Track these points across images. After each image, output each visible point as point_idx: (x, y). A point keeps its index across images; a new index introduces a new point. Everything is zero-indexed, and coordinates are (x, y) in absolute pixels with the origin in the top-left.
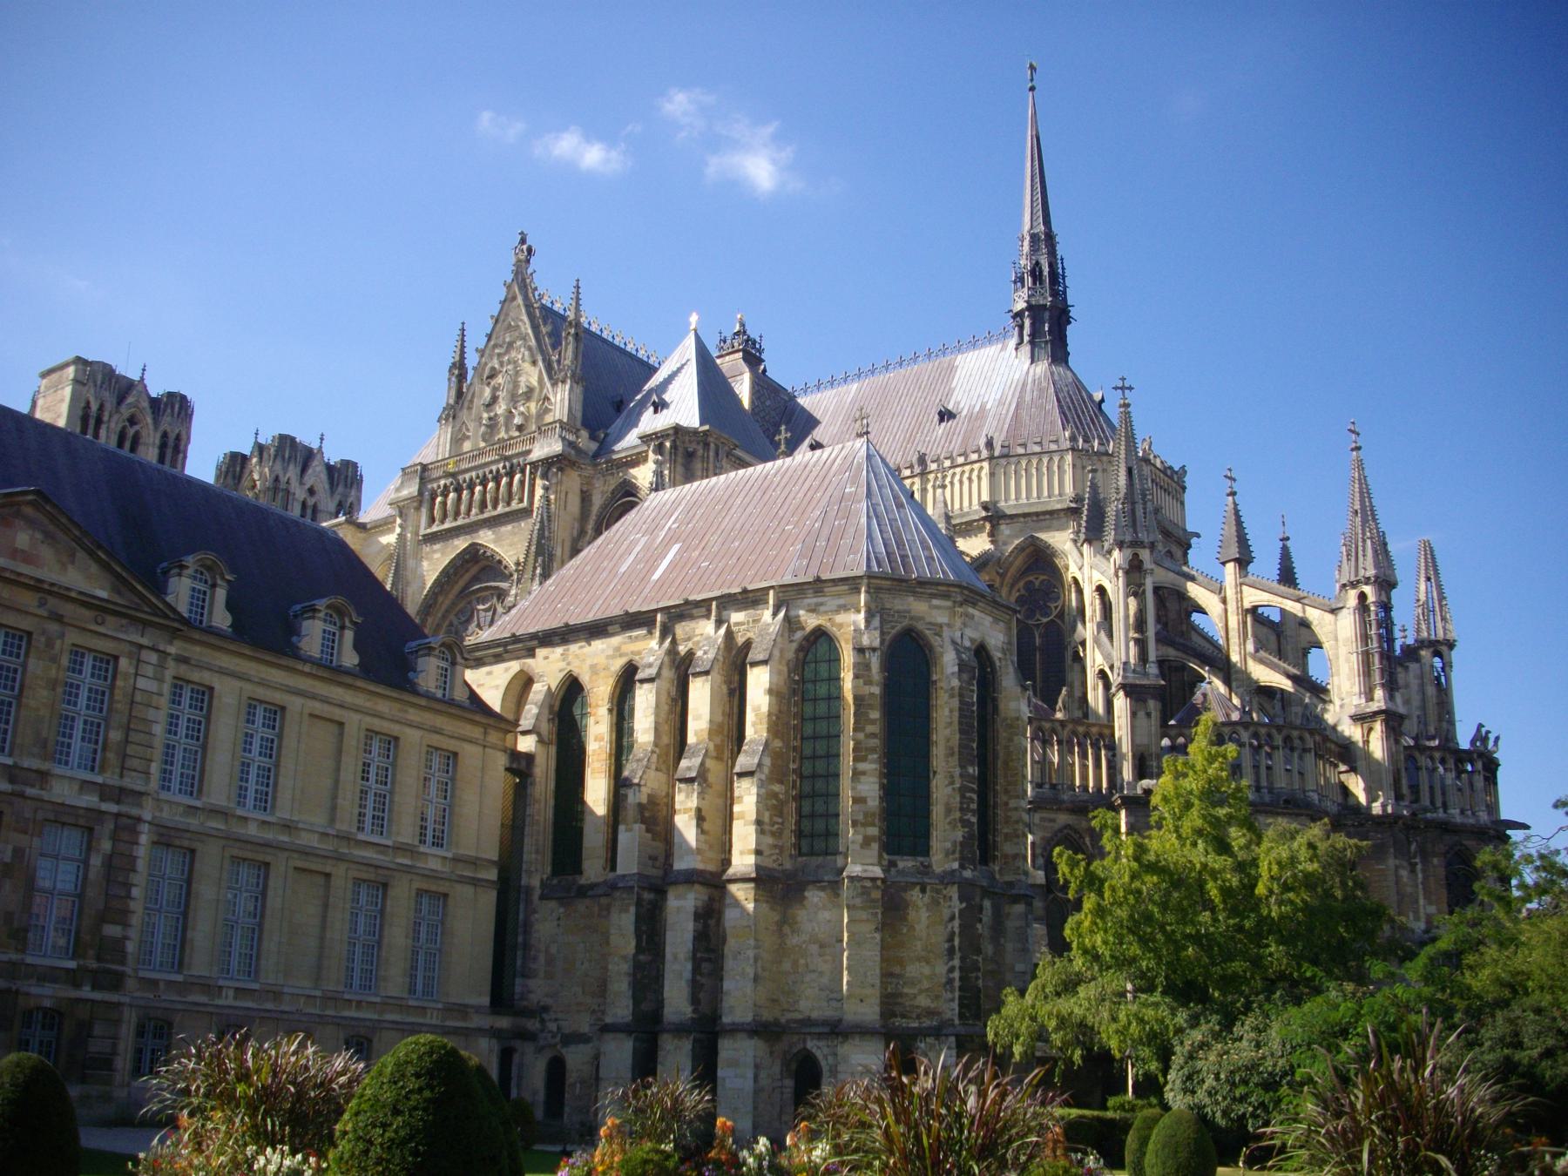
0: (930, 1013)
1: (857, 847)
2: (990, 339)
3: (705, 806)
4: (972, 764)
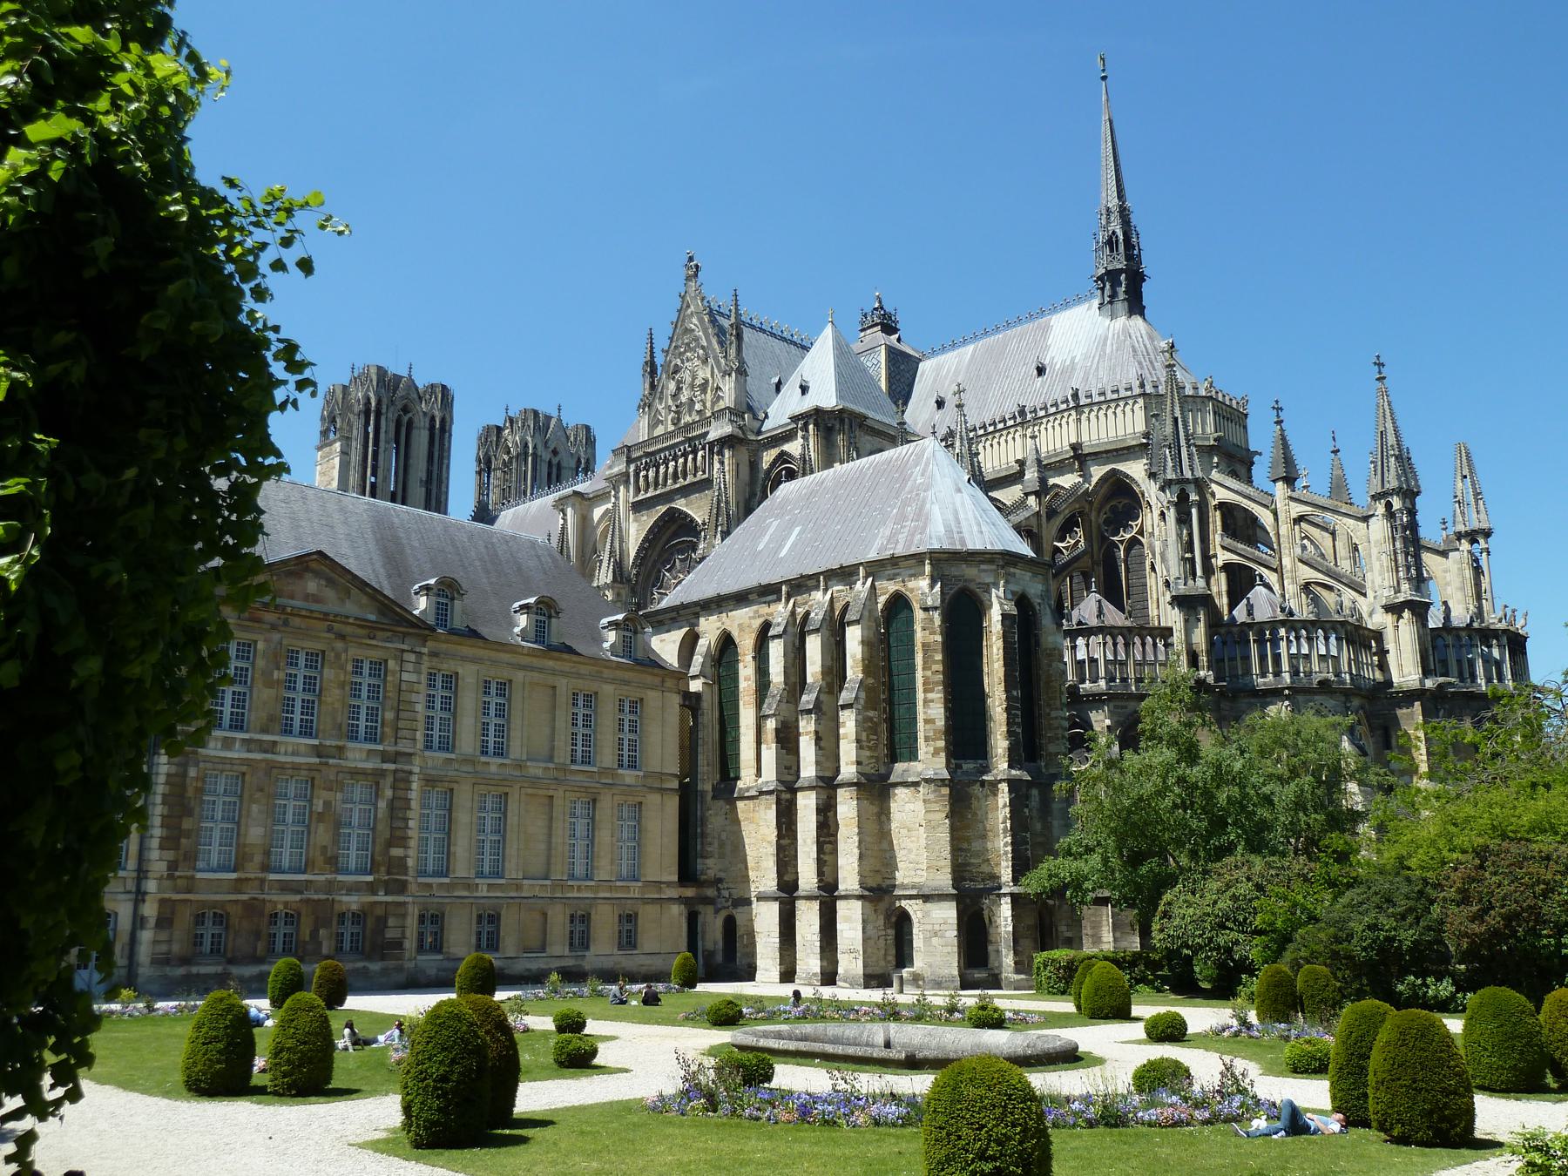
2: (1079, 300)
3: (820, 729)
4: (1016, 689)
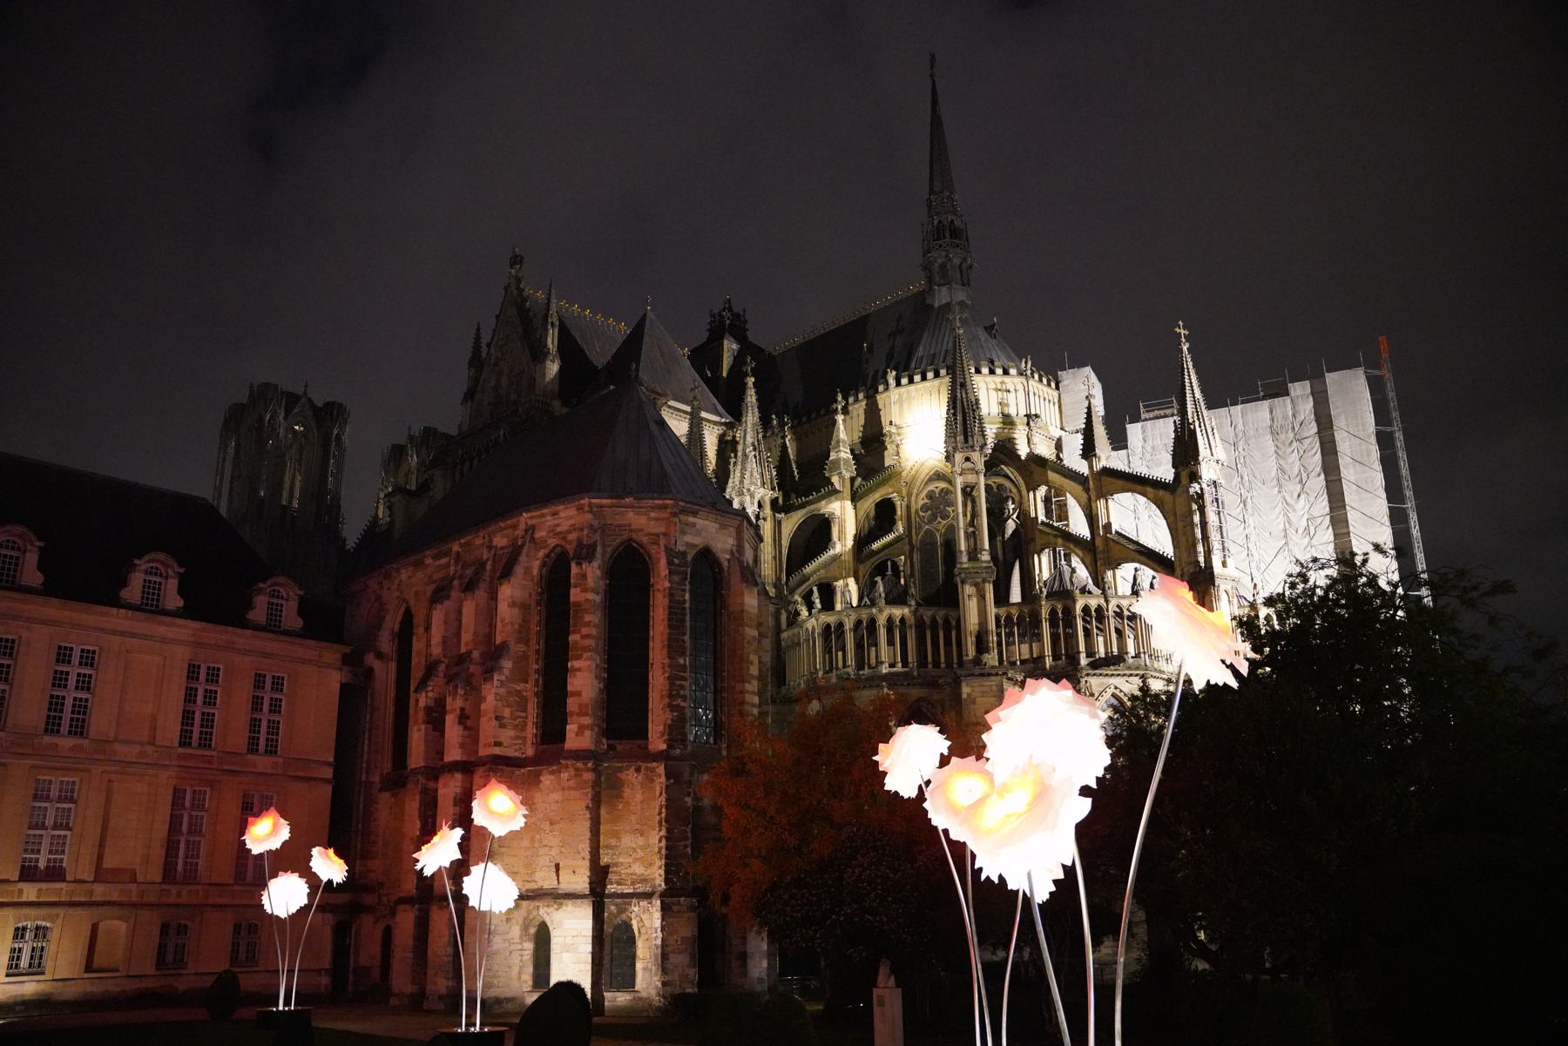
0: (644, 881)
1: (573, 735)
4: (683, 654)
